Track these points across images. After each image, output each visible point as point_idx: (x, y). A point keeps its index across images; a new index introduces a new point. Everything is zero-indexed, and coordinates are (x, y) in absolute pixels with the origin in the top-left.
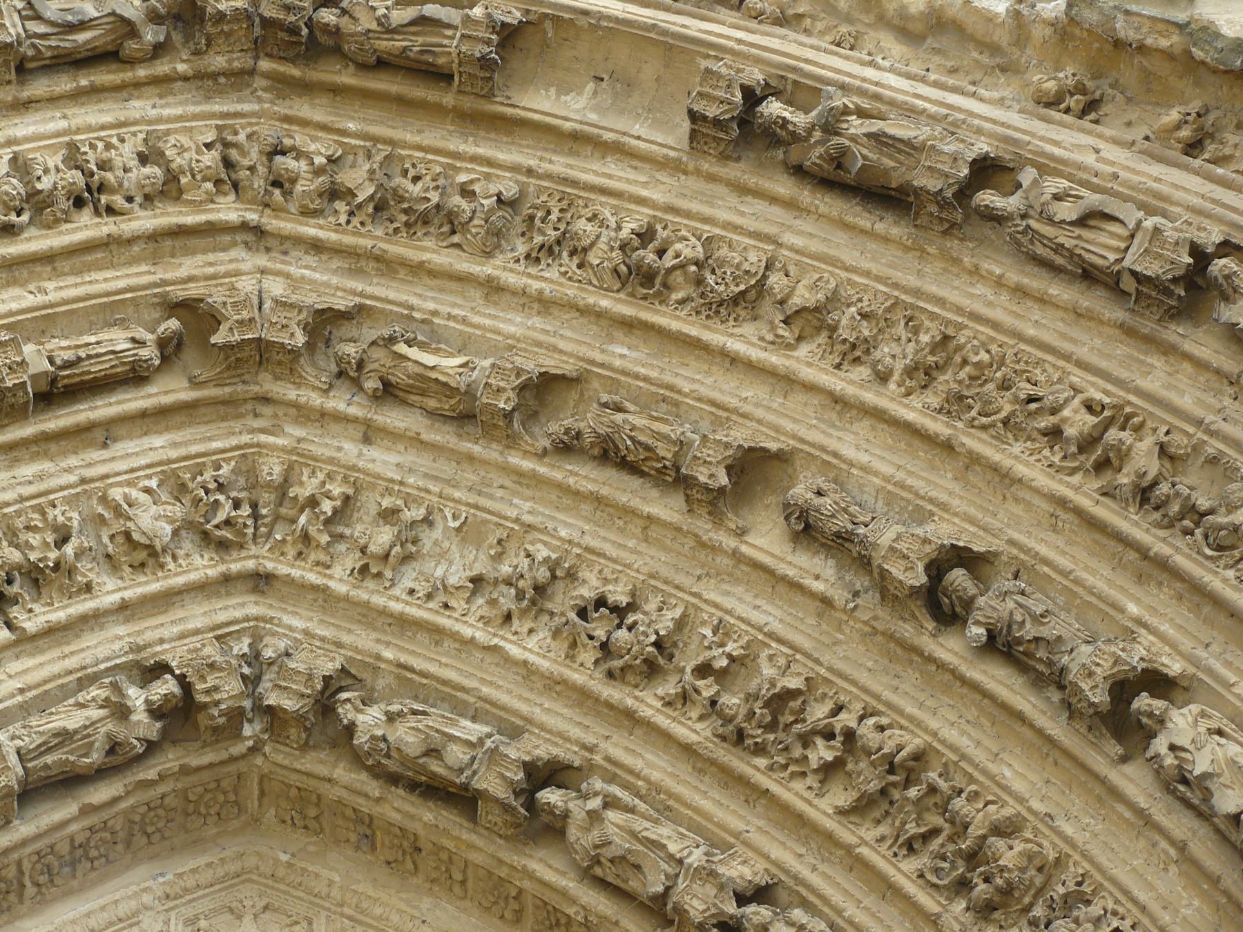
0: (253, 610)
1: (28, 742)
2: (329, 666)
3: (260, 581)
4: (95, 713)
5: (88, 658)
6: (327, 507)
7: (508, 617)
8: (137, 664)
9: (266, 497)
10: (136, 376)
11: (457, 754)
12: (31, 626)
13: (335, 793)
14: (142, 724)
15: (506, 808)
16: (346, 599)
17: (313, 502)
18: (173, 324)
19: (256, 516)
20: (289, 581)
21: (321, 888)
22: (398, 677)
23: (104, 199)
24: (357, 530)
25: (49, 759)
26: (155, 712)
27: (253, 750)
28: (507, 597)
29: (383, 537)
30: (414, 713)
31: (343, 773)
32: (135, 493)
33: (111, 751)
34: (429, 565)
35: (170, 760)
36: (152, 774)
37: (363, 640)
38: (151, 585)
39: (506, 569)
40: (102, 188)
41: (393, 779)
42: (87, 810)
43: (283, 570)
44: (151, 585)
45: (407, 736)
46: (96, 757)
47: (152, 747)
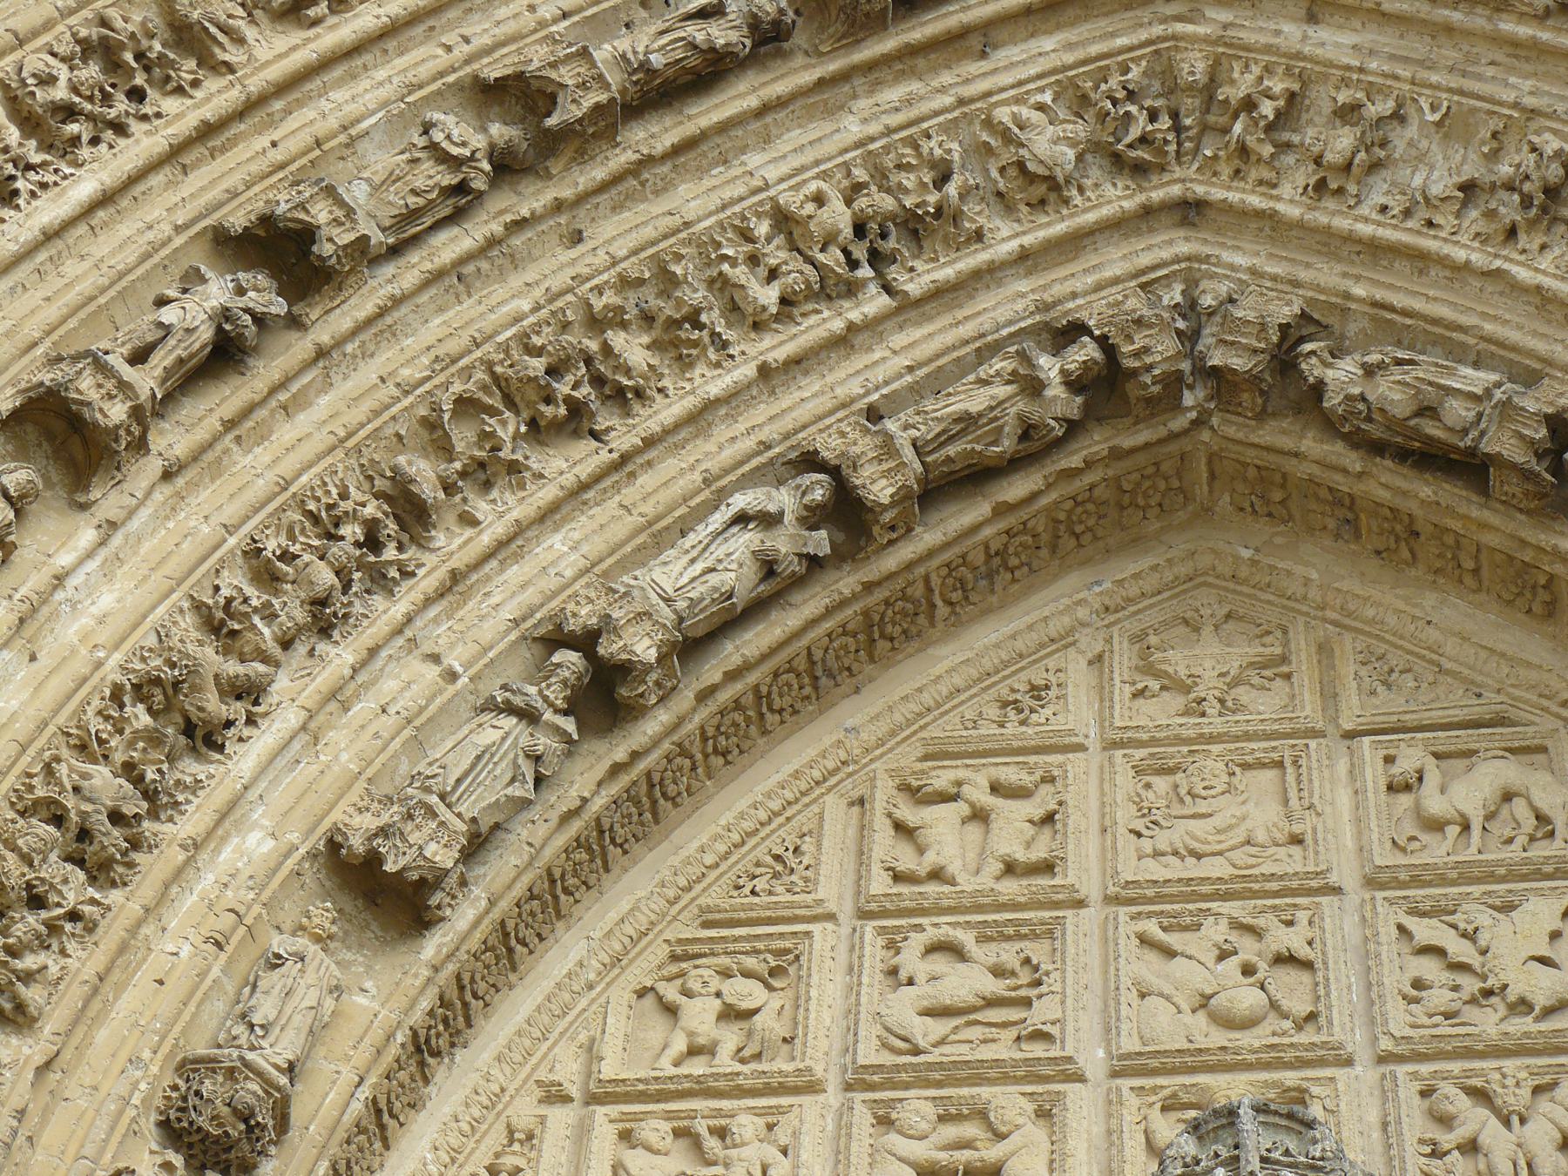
0: (1184, 248)
1: (924, 432)
2: (1285, 312)
3: (1190, 211)
4: (1002, 391)
5: (985, 322)
6: (1267, 109)
7: (1512, 233)
8: (1046, 326)
9: (1189, 103)
11: (1458, 411)
12: (914, 288)
13: (1303, 470)
14: (1059, 401)
15: (1527, 475)
16: (1300, 225)
17: (1249, 105)
19: (1177, 128)
20: (1227, 208)
21: (1295, 588)
22: (1373, 319)
24: (1309, 135)
25: (952, 450)
26: (1074, 384)
27: (1197, 423)
28: (1509, 209)
29: (1343, 141)
30: (1399, 362)
31: (1312, 444)
32: (1025, 112)
33: (1025, 436)
34: (1403, 173)
35: (1096, 442)
36: (1075, 461)
37: (1326, 275)
38: (1055, 227)
39: (1505, 170)
41: (1377, 448)
42: (1001, 510)
43: (1217, 194)
44: (1055, 227)
45: (1391, 393)
46: (1007, 445)
47: (1073, 428)
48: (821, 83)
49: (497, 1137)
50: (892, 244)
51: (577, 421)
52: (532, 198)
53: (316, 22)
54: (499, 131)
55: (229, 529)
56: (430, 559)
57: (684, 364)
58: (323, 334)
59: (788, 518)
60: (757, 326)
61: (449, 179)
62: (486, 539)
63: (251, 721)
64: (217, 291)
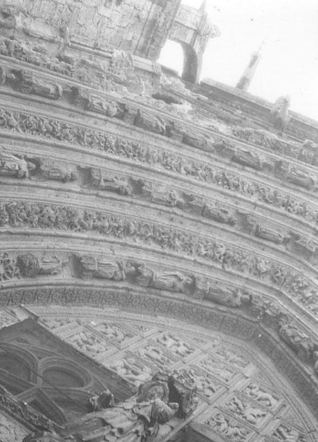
6: (301, 285)
10: (277, 242)
12: (227, 269)
14: (237, 301)
16: (294, 304)
17: (298, 282)
18: (289, 236)
19: (285, 279)
20: (285, 296)
22: (296, 322)
23: (289, 208)
25: (215, 294)
26: (242, 300)
30: (295, 328)
32: (262, 261)
35: (239, 312)
36: (234, 312)
38: (255, 279)
40: (290, 205)
47: (237, 307)
48: (234, 233)
49: (65, 318)
50: (229, 261)
51: (161, 242)
52: (178, 211)
53: (167, 169)
54: (182, 200)
55: (98, 208)
56: (124, 239)
57: (184, 250)
58: (134, 201)
59: (182, 282)
60: (199, 255)
61: (170, 200)
62: (134, 244)
63: (79, 230)
64: (125, 183)
